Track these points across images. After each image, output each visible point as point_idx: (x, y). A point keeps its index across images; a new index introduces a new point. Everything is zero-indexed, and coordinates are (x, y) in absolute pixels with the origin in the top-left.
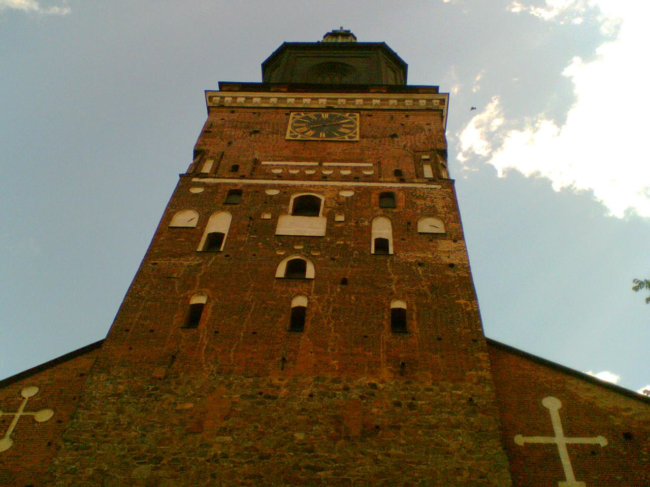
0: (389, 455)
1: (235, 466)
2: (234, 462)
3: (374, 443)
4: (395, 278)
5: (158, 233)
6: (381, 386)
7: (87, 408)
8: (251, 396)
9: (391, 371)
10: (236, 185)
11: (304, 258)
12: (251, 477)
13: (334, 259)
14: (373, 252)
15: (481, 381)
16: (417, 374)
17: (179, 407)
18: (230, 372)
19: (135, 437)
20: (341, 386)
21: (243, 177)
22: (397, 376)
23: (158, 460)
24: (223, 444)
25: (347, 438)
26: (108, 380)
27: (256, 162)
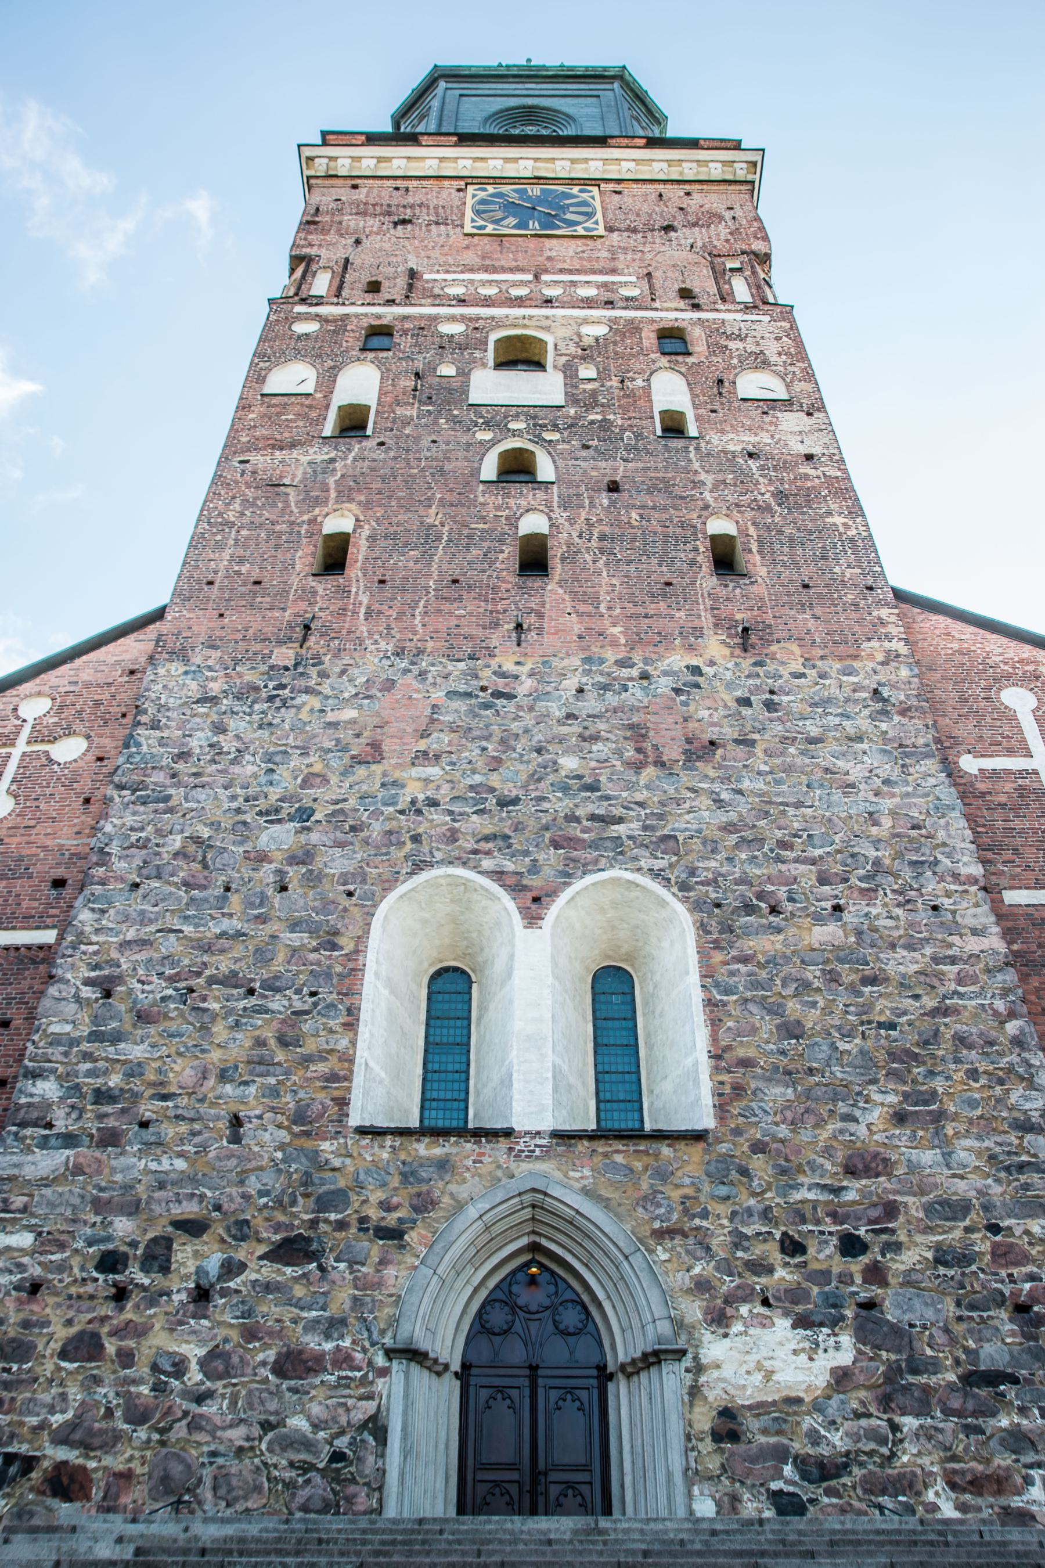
0: (740, 792)
1: (454, 820)
2: (451, 813)
3: (712, 773)
7: (155, 726)
8: (469, 695)
9: (723, 642)
11: (530, 446)
12: (487, 838)
13: (588, 447)
16: (774, 648)
17: (331, 717)
18: (420, 652)
19: (255, 776)
20: (635, 673)
21: (391, 302)
22: (738, 651)
23: (304, 814)
24: (427, 781)
25: (660, 764)
26: (186, 673)
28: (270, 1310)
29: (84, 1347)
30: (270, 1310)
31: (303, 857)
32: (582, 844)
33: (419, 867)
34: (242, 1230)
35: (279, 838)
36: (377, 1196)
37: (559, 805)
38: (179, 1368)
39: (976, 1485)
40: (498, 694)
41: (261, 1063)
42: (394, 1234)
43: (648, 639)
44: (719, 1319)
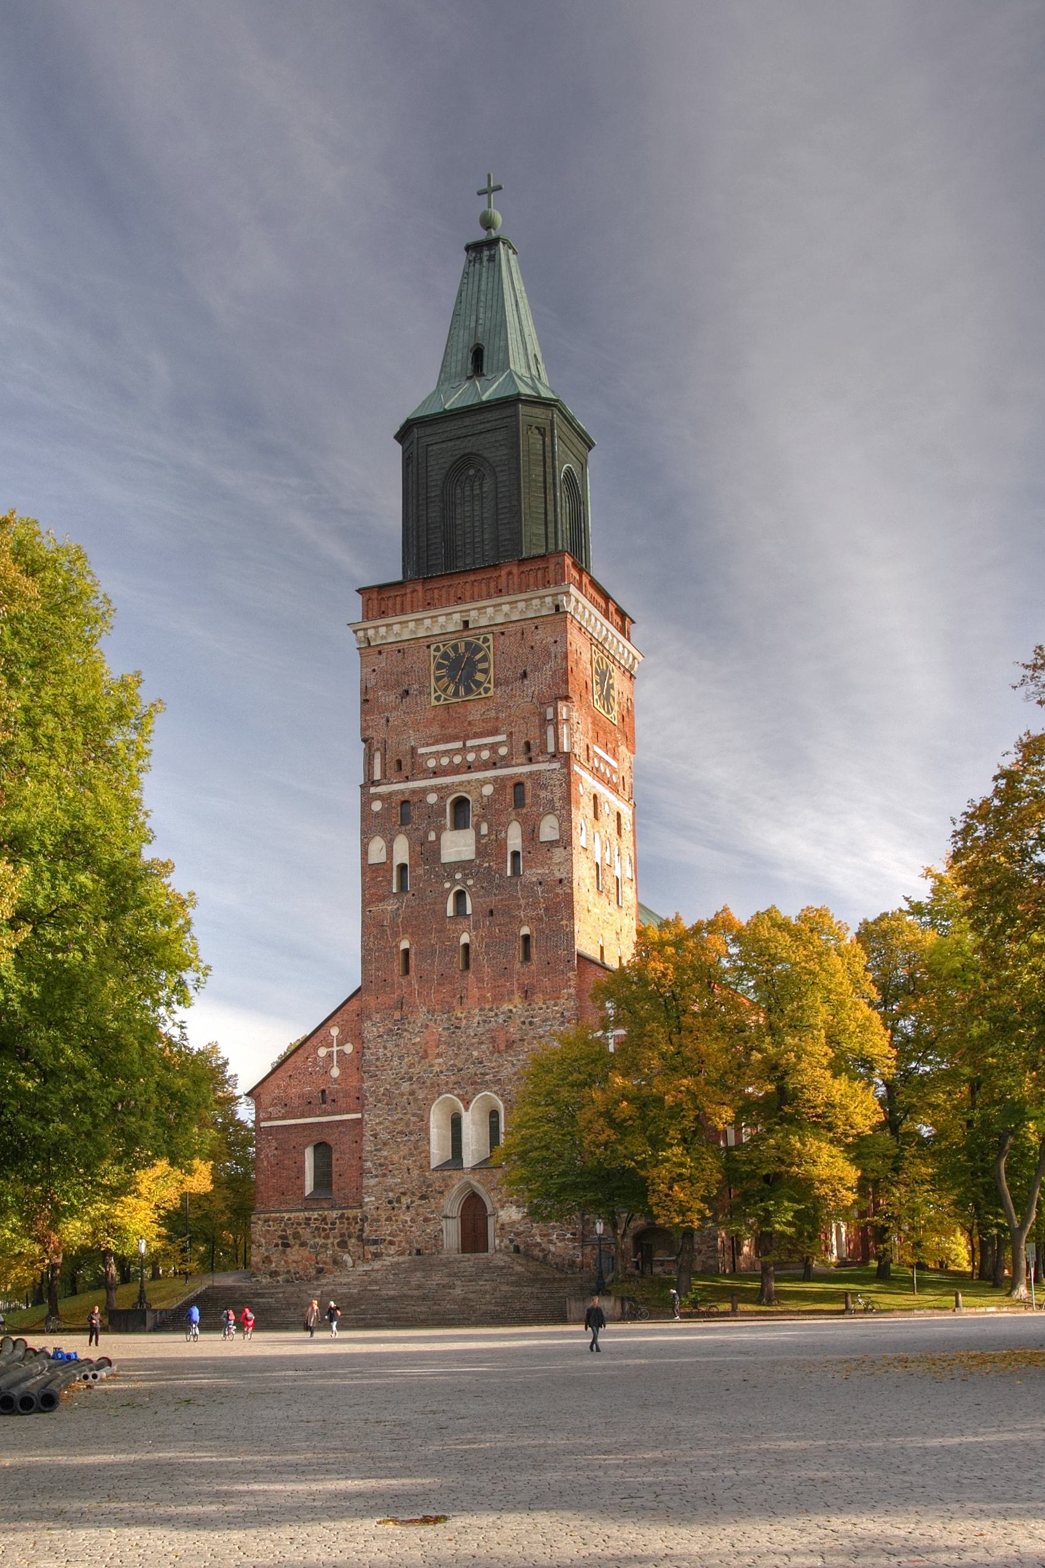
4: (522, 902)
5: (363, 874)
6: (514, 1010)
8: (448, 1029)
10: (402, 792)
14: (509, 873)
15: (570, 995)
18: (434, 1011)
23: (411, 1079)
27: (413, 750)
28: (421, 1210)
29: (389, 1219)
30: (421, 1210)
31: (412, 1093)
32: (477, 1083)
33: (440, 1094)
34: (413, 1194)
35: (405, 1087)
36: (438, 1184)
37: (473, 1069)
38: (406, 1222)
39: (545, 1235)
40: (457, 1028)
41: (412, 1155)
42: (441, 1193)
43: (498, 999)
44: (502, 1207)
